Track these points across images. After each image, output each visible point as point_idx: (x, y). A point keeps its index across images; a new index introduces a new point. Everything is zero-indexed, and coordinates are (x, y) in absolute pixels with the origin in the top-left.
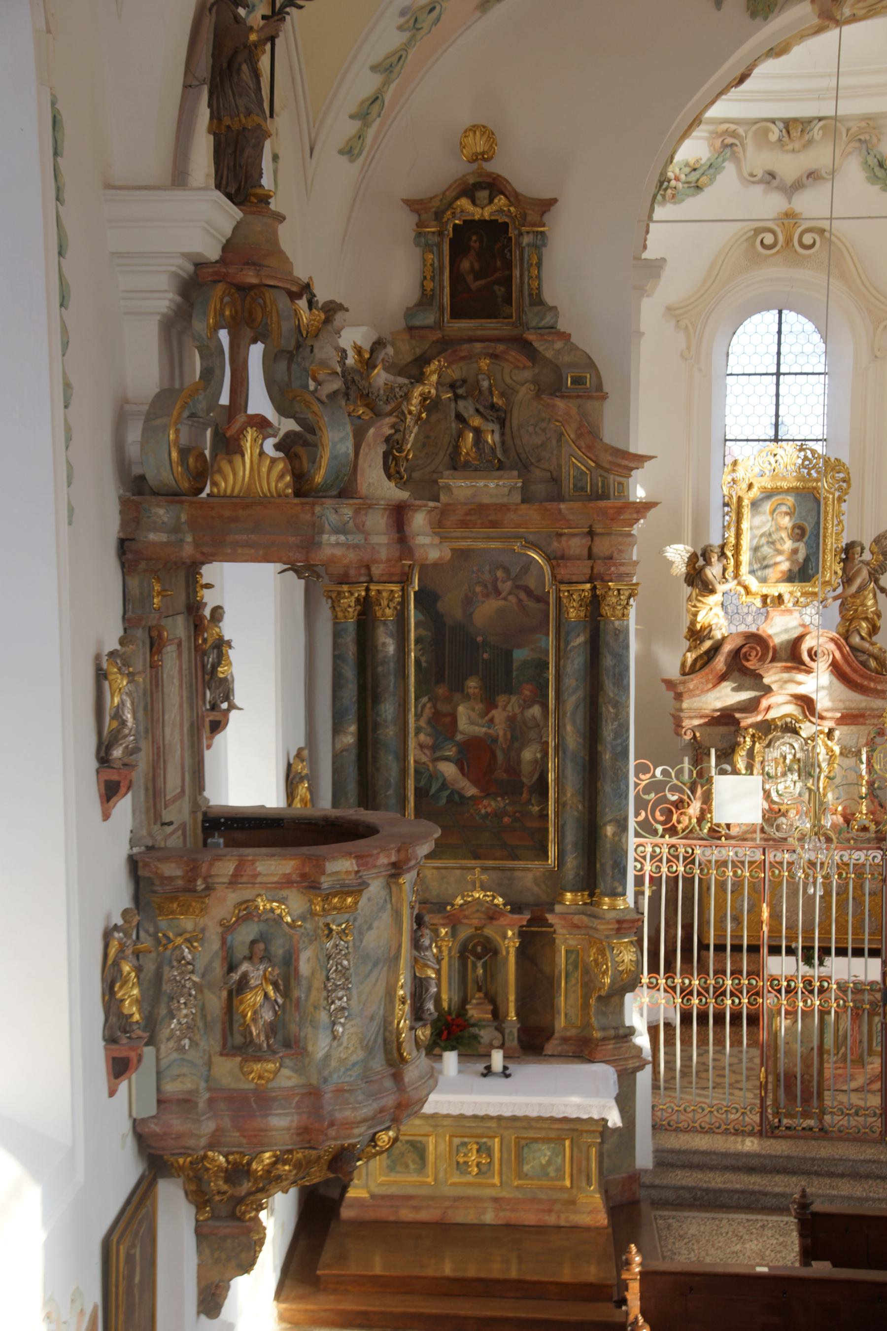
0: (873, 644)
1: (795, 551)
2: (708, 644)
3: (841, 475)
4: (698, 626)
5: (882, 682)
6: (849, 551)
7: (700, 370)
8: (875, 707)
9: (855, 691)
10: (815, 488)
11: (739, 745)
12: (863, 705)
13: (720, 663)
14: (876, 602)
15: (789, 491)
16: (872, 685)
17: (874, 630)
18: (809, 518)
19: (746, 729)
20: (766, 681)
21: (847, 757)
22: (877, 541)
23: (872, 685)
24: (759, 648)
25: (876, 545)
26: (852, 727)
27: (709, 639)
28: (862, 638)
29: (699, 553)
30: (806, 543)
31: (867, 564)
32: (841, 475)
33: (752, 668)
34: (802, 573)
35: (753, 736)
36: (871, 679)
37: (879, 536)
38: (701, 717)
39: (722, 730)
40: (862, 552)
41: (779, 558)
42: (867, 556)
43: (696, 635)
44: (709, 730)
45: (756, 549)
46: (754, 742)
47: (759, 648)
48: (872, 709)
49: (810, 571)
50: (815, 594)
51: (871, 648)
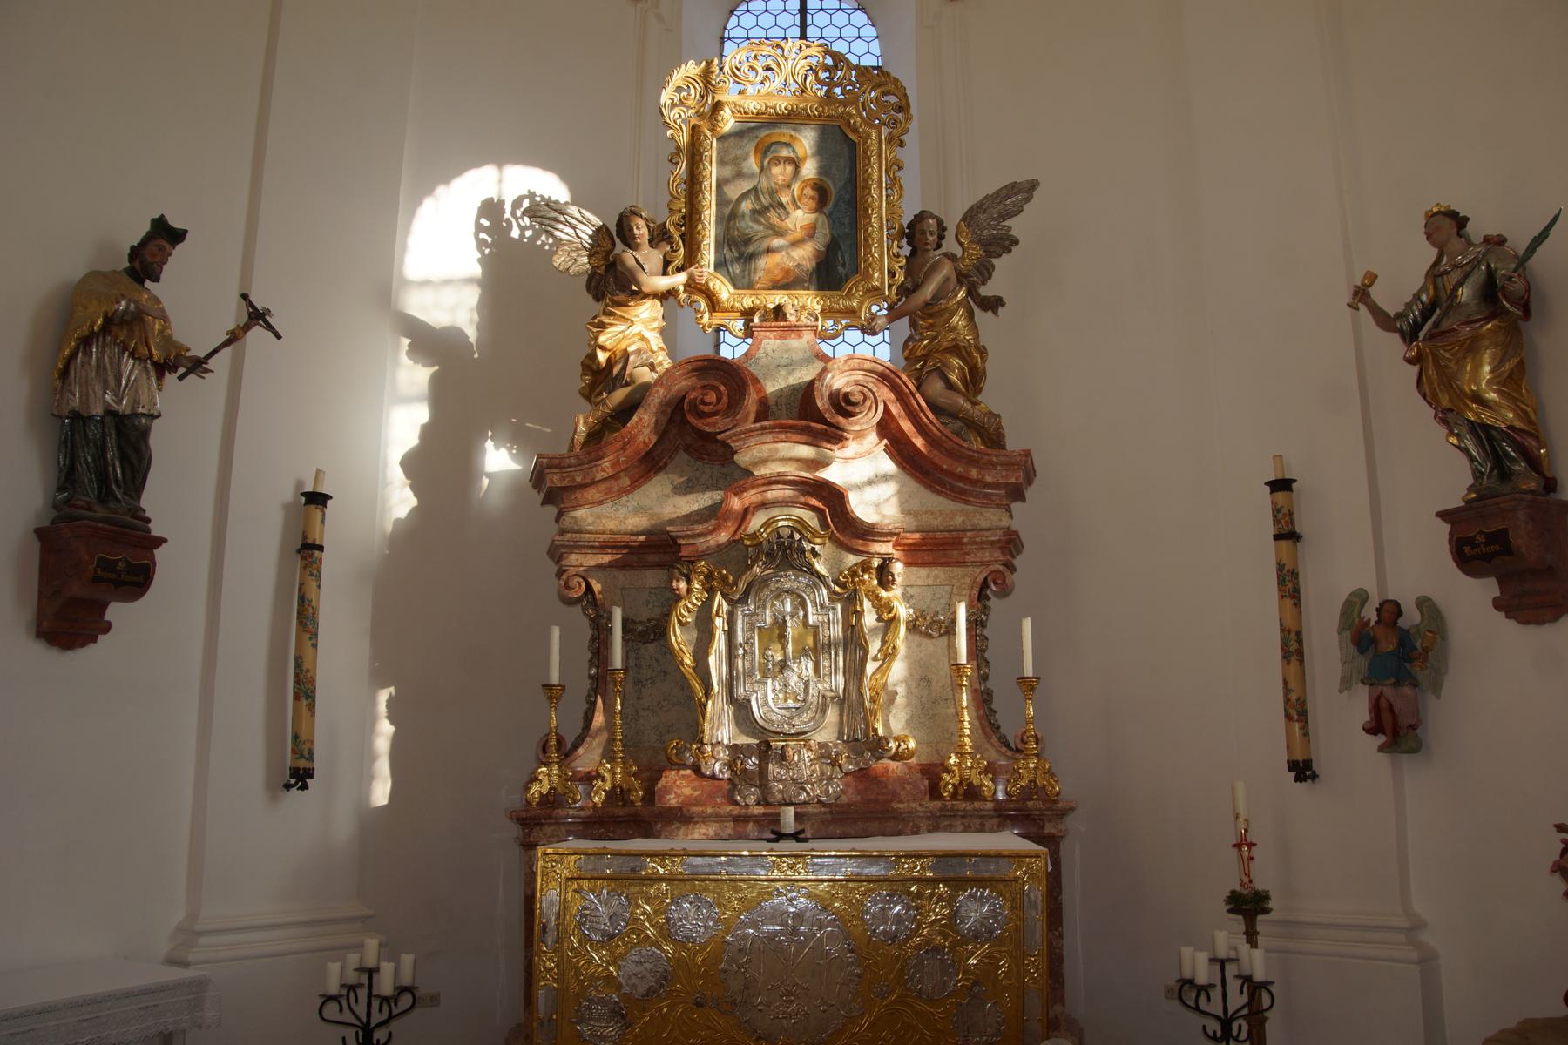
0: (974, 404)
1: (811, 232)
2: (620, 395)
3: (893, 99)
4: (602, 357)
5: (994, 465)
6: (915, 234)
7: (660, 18)
8: (984, 524)
9: (938, 492)
10: (840, 117)
11: (679, 598)
12: (958, 520)
13: (643, 425)
14: (974, 329)
15: (791, 118)
16: (974, 473)
17: (974, 379)
18: (834, 170)
19: (692, 562)
20: (742, 458)
21: (930, 636)
22: (969, 217)
23: (974, 473)
24: (722, 388)
25: (968, 226)
26: (936, 571)
27: (627, 384)
28: (950, 386)
29: (613, 230)
30: (830, 216)
31: (952, 257)
32: (893, 99)
33: (708, 429)
34: (832, 271)
35: (709, 577)
36: (972, 462)
37: (971, 209)
38: (604, 548)
39: (652, 578)
40: (941, 237)
41: (777, 242)
42: (950, 245)
43: (602, 377)
44: (622, 577)
45: (728, 217)
46: (711, 591)
47: (722, 388)
48: (975, 529)
49: (840, 269)
50: (852, 312)
51: (968, 406)
